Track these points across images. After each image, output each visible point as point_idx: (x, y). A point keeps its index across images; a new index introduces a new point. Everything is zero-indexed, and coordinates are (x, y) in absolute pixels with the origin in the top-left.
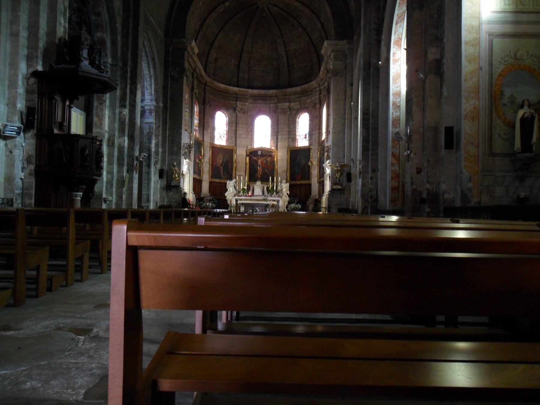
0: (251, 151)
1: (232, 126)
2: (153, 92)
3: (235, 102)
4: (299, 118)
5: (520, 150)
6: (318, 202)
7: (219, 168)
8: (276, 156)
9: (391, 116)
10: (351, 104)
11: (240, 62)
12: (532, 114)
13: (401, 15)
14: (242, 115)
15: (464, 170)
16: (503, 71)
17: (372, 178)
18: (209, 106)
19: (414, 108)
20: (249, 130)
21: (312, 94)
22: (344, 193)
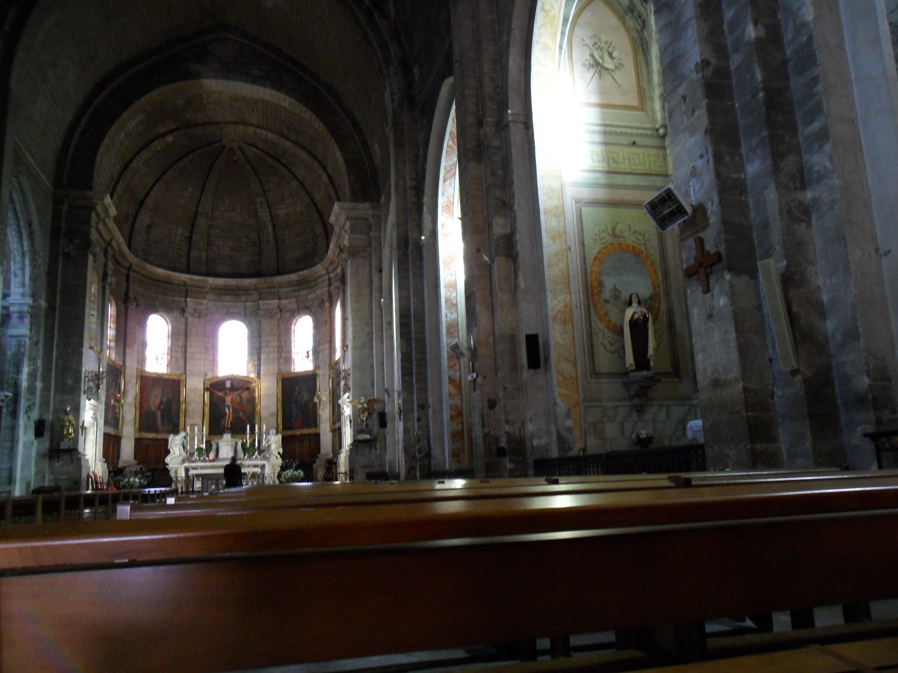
0: (212, 382)
1: (178, 339)
2: (27, 281)
3: (183, 299)
4: (295, 324)
5: (634, 367)
6: (332, 464)
7: (154, 414)
8: (258, 388)
9: (444, 320)
10: (380, 300)
11: (191, 233)
12: (643, 314)
13: (450, 169)
14: (197, 320)
15: (558, 400)
16: (600, 252)
17: (419, 420)
18: (137, 306)
19: (478, 307)
20: (209, 345)
21: (316, 285)
22: (376, 446)
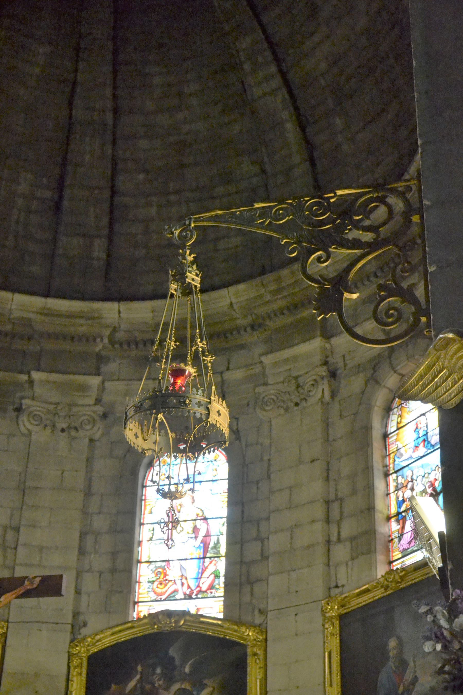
3: (24, 377)
